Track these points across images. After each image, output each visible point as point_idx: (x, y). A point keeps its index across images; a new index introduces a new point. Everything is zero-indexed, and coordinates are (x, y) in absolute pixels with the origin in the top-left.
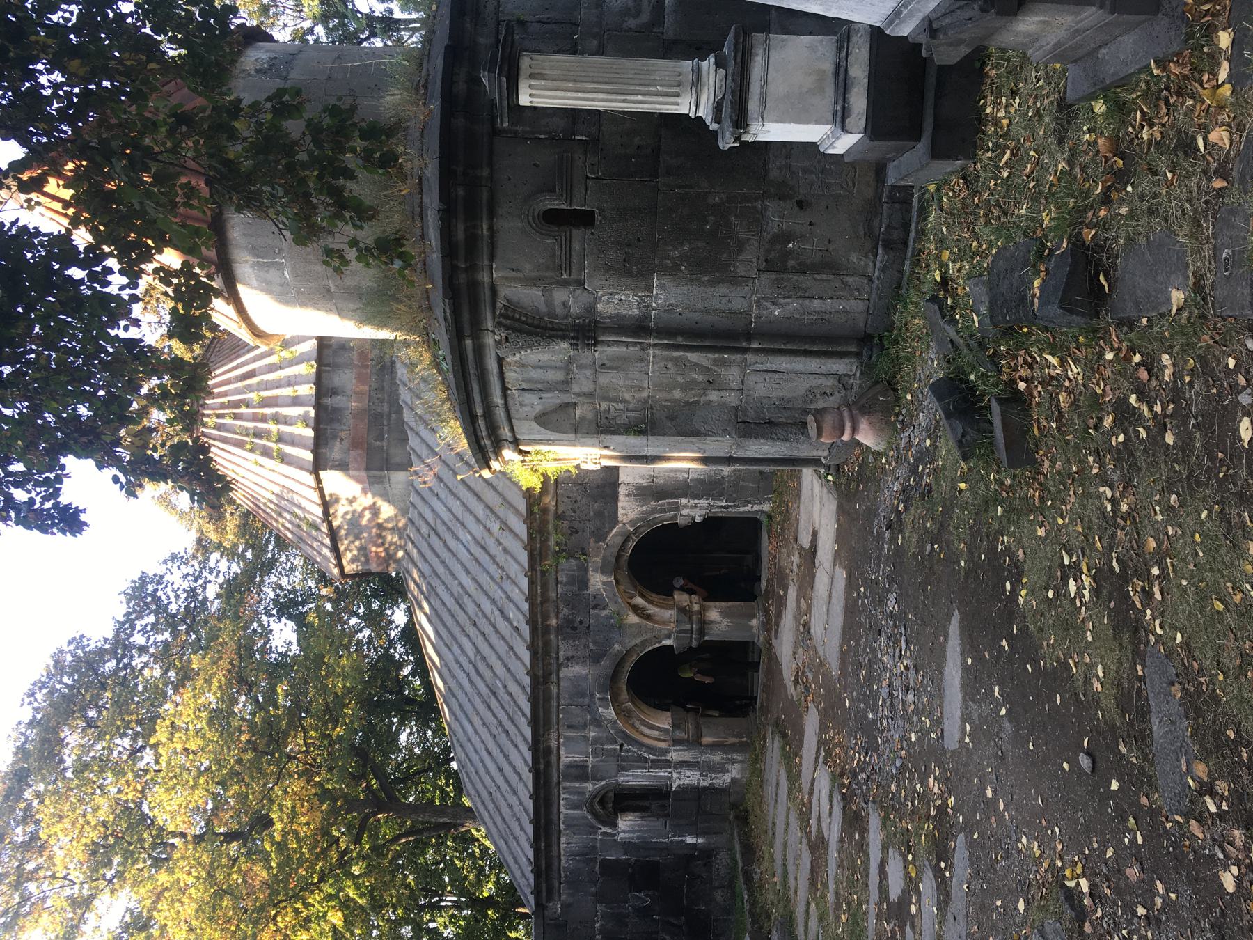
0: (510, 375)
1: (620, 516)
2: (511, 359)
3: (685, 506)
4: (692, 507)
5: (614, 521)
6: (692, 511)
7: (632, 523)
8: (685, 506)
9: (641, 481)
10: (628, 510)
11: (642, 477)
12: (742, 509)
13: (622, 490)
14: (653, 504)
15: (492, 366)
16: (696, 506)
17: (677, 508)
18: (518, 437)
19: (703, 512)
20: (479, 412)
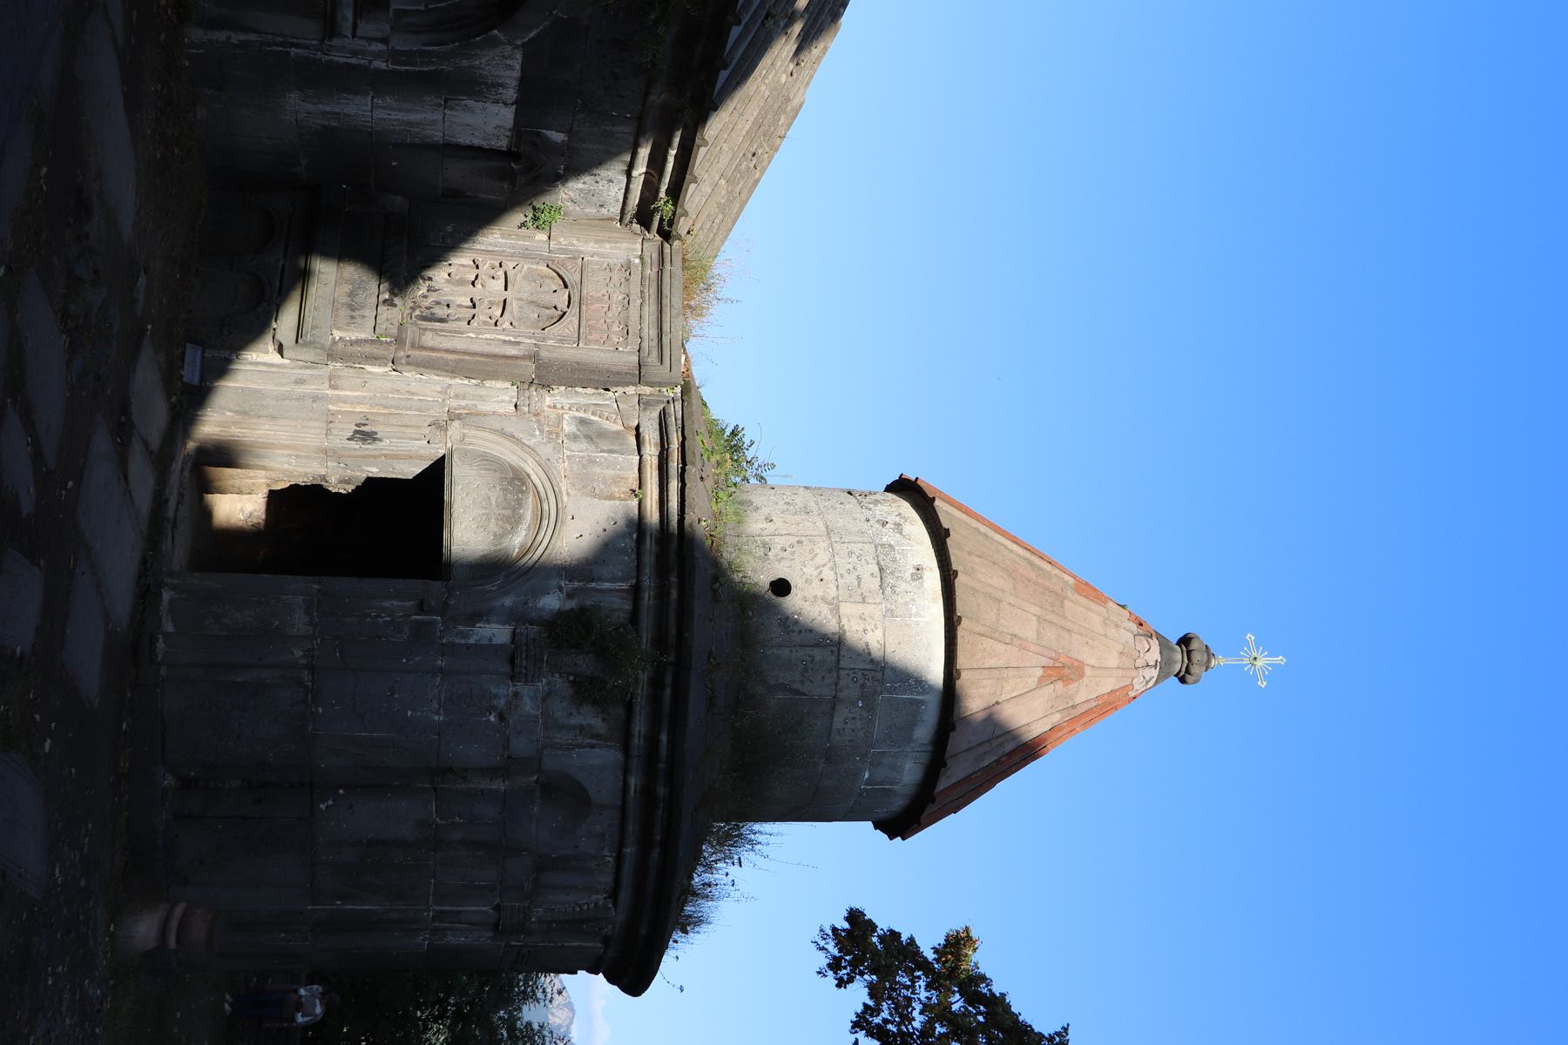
0: (606, 879)
1: (519, 56)
2: (600, 898)
3: (378, 55)
4: (363, 53)
5: (531, 54)
6: (365, 43)
7: (495, 43)
8: (378, 55)
9: (471, 103)
10: (505, 65)
11: (466, 108)
12: (252, 37)
13: (511, 94)
14: (446, 67)
15: (625, 896)
16: (354, 53)
17: (395, 56)
18: (620, 756)
19: (336, 42)
20: (656, 853)
